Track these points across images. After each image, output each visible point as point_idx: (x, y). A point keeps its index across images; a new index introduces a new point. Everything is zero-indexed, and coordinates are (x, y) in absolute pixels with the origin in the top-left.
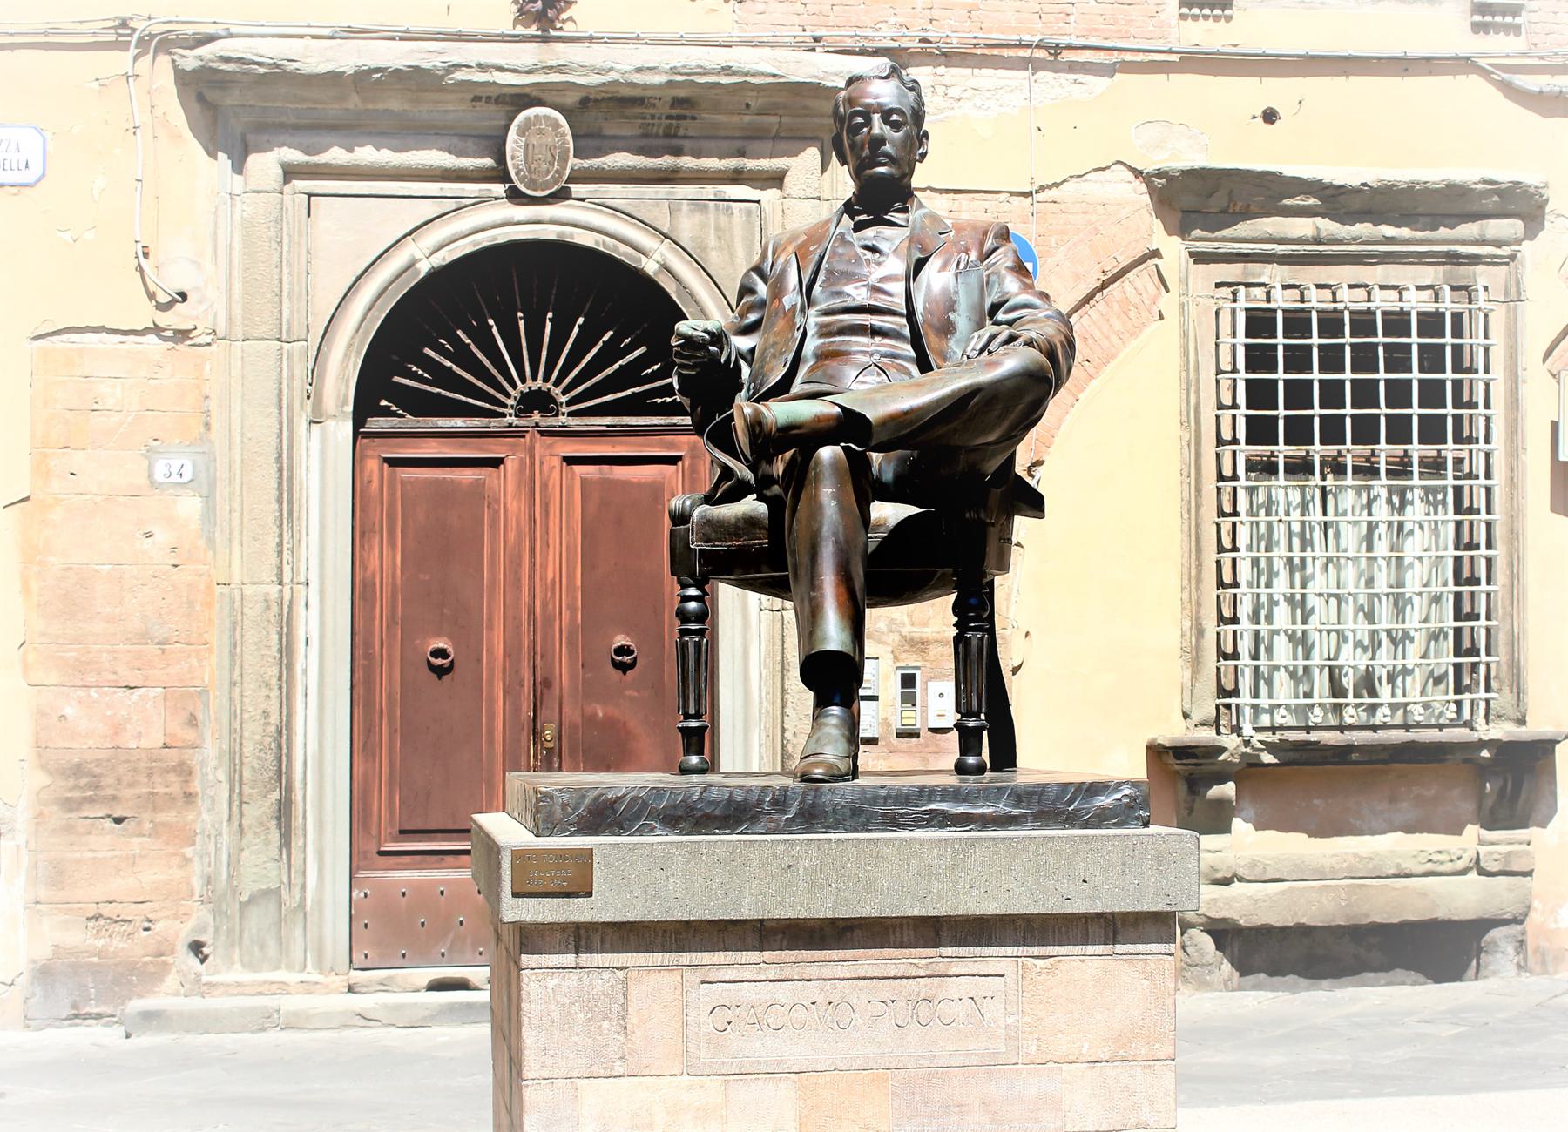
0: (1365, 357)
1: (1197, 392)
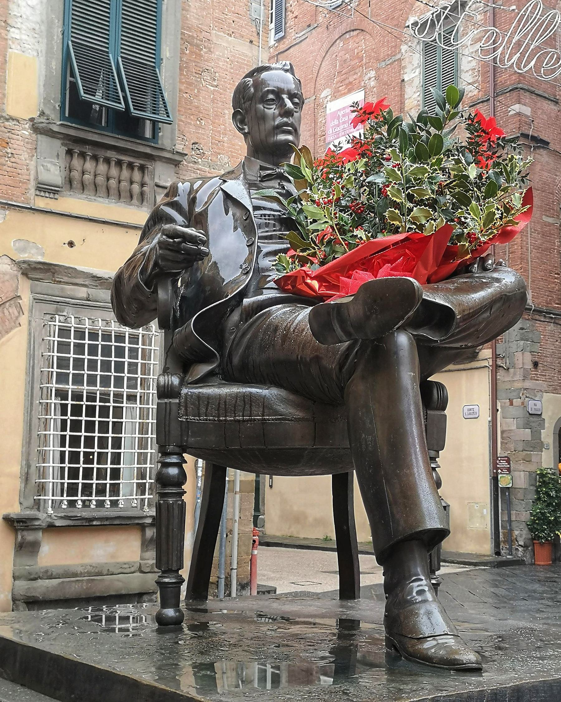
0: (106, 351)
1: (34, 360)
